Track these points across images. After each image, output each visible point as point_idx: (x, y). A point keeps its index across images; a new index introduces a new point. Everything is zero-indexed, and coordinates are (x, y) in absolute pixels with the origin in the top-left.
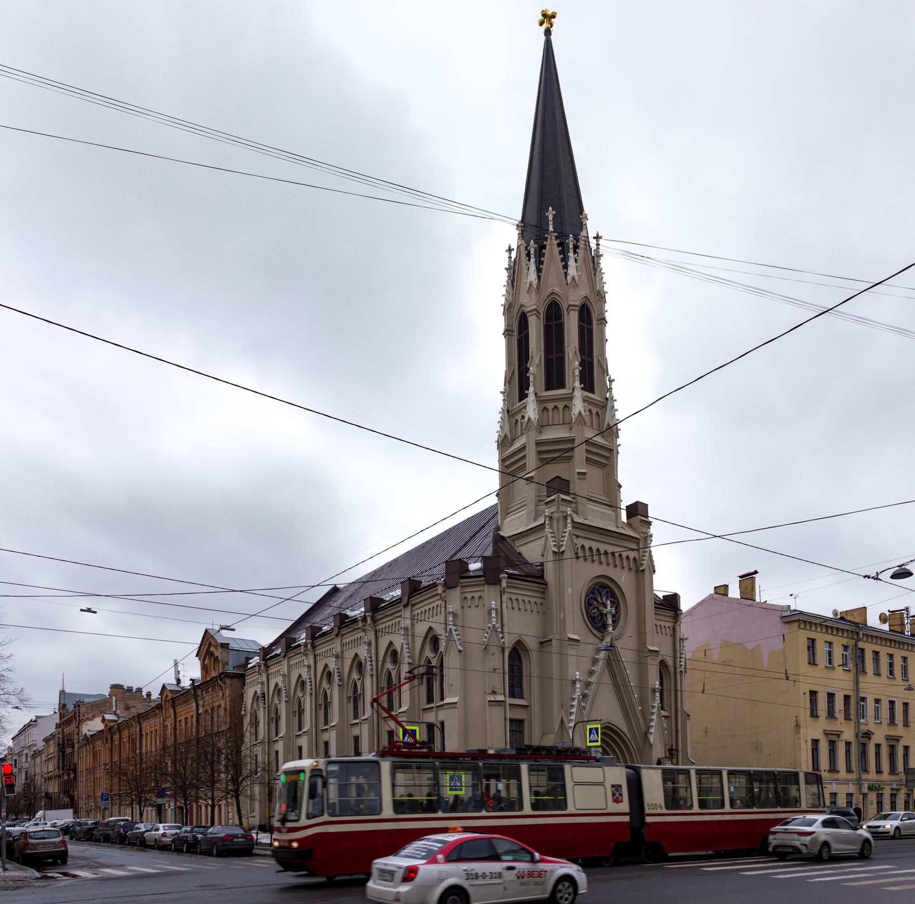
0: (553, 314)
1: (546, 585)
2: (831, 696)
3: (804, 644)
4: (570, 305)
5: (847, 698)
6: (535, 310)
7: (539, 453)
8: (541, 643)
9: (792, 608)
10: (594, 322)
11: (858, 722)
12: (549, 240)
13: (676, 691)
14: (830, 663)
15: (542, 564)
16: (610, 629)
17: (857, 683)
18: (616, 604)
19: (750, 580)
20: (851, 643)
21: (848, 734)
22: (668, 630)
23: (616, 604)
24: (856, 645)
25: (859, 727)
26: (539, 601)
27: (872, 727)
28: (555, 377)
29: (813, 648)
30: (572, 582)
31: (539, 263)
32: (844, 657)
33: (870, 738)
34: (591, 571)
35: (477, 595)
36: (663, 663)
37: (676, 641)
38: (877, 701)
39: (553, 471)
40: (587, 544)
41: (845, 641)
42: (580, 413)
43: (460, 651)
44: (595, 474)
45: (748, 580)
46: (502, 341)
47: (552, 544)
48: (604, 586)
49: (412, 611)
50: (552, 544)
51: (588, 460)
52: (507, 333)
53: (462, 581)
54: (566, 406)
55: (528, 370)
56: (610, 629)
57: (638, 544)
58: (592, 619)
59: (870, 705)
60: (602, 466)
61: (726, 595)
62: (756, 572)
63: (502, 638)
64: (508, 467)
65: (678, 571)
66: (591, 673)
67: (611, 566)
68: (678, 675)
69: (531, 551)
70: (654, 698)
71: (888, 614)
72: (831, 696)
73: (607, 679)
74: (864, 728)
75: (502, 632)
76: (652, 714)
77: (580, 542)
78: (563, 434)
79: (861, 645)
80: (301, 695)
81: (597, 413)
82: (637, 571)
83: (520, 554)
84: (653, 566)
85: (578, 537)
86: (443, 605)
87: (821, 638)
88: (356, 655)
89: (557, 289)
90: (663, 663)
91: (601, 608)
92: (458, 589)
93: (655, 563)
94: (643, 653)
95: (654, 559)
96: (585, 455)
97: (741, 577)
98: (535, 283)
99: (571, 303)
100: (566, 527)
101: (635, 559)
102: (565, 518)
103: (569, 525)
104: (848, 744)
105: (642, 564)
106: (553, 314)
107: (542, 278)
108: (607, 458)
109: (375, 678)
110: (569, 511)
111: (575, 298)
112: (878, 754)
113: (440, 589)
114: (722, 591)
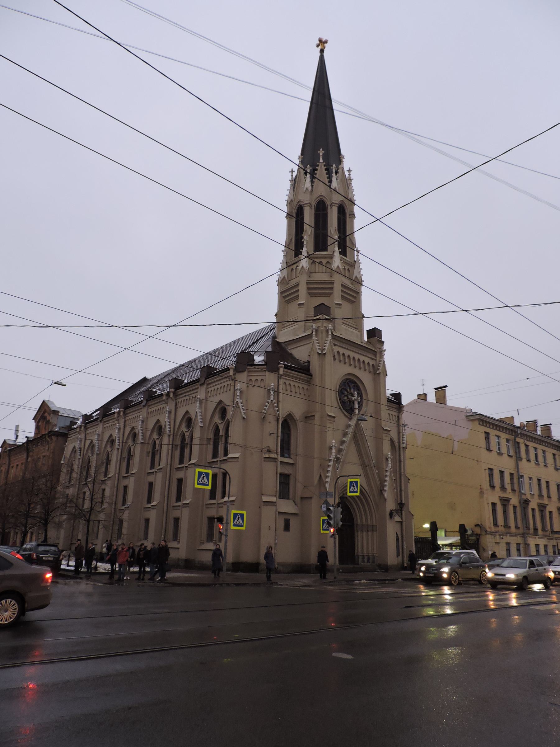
0: (321, 208)
1: (311, 375)
2: (502, 472)
3: (483, 436)
4: (332, 203)
5: (511, 474)
6: (310, 203)
7: (309, 289)
8: (306, 417)
9: (473, 411)
10: (347, 215)
11: (520, 492)
12: (320, 166)
13: (400, 461)
14: (499, 450)
15: (309, 362)
16: (357, 411)
17: (517, 465)
18: (360, 394)
19: (442, 391)
20: (511, 437)
21: (514, 501)
22: (394, 417)
23: (360, 394)
24: (515, 440)
25: (521, 497)
26: (306, 387)
27: (528, 496)
28: (321, 243)
29: (488, 438)
30: (331, 374)
31: (313, 177)
32: (508, 447)
33: (528, 504)
34: (343, 370)
35: (259, 378)
36: (392, 441)
37: (399, 425)
38: (530, 479)
39: (317, 301)
40: (342, 351)
41: (508, 436)
42: (338, 267)
43: (244, 418)
44: (346, 306)
45: (441, 391)
46: (285, 221)
47: (318, 347)
48: (352, 381)
49: (207, 389)
50: (318, 347)
51: (342, 296)
52: (289, 216)
53: (249, 367)
54: (328, 262)
55: (302, 238)
56: (357, 411)
57: (375, 355)
58: (343, 403)
59: (526, 480)
60: (352, 302)
61: (425, 400)
62: (446, 386)
63: (278, 411)
64: (284, 297)
65: (405, 374)
66: (342, 442)
67: (357, 368)
68: (402, 449)
69: (300, 353)
70: (387, 464)
71: (525, 423)
72: (502, 472)
73: (353, 448)
74: (524, 497)
75: (278, 406)
76: (386, 476)
77: (336, 349)
78: (325, 277)
79: (518, 440)
80: (109, 449)
81: (348, 269)
82: (375, 373)
83: (291, 354)
84: (386, 371)
85: (335, 345)
86: (233, 384)
87: (493, 432)
88: (158, 421)
89: (323, 194)
90: (392, 441)
91: (350, 397)
92: (246, 373)
93: (387, 369)
94: (380, 430)
95: (386, 366)
96: (341, 293)
97: (436, 389)
98: (310, 188)
99: (333, 202)
100: (327, 337)
101: (373, 365)
102: (327, 331)
103: (330, 336)
104: (515, 507)
105: (378, 369)
106: (321, 208)
107: (314, 187)
108: (355, 297)
109: (171, 437)
110: (330, 326)
111: (337, 199)
112: (534, 516)
113: (231, 372)
114: (423, 397)
